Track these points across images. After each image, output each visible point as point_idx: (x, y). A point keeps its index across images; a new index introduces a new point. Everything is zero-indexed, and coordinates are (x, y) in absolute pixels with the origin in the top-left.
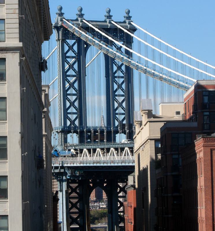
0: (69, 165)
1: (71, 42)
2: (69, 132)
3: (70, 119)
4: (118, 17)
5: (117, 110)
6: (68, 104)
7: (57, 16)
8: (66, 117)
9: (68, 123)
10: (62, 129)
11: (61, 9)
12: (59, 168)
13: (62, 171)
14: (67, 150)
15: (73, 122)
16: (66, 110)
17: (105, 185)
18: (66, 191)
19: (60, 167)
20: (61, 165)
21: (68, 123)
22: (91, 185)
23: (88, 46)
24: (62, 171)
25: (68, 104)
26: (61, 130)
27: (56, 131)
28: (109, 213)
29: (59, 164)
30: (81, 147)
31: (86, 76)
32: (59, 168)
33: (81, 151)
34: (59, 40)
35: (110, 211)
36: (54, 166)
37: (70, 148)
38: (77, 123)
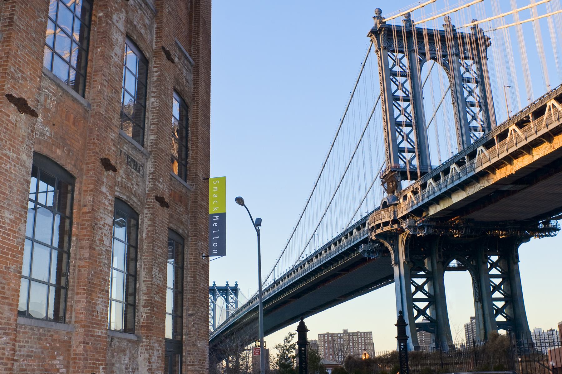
0: (405, 213)
9: (401, 162)
10: (391, 168)
11: (379, 11)
12: (390, 223)
14: (402, 197)
18: (404, 262)
20: (392, 218)
24: (396, 226)
28: (477, 302)
29: (390, 217)
31: (424, 98)
32: (390, 223)
33: (424, 186)
34: (380, 49)
35: (477, 298)
36: (383, 223)
38: (415, 162)
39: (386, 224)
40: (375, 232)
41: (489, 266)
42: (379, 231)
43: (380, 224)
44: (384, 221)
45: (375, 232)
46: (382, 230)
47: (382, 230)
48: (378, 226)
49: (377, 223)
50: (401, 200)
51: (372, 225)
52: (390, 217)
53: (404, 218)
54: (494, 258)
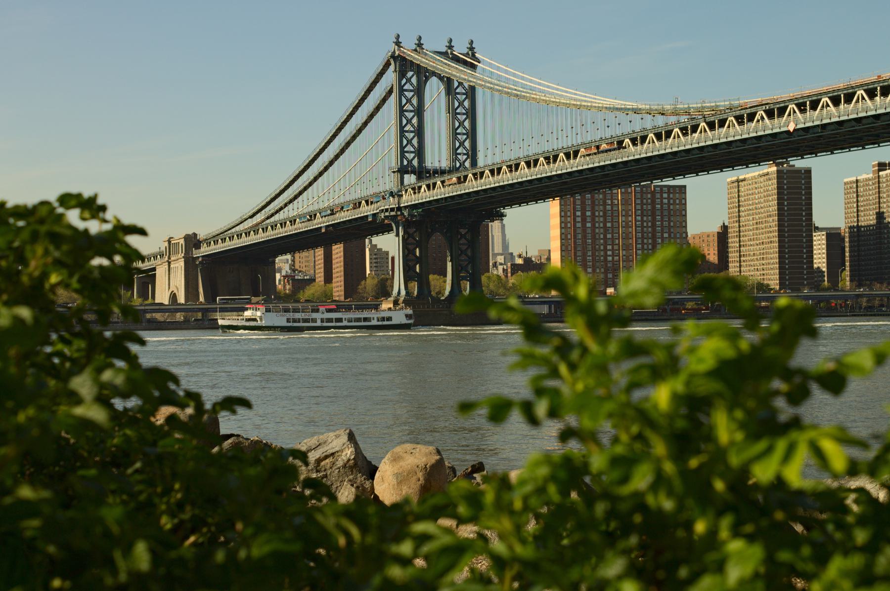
0: (406, 204)
2: (407, 172)
3: (406, 159)
4: (460, 49)
5: (464, 138)
6: (405, 142)
7: (394, 44)
8: (403, 156)
9: (405, 163)
15: (410, 162)
16: (402, 148)
17: (445, 231)
21: (405, 163)
22: (430, 230)
23: (427, 79)
25: (405, 142)
26: (397, 170)
27: (392, 171)
29: (396, 205)
30: (420, 184)
36: (391, 208)
37: (407, 188)
38: (415, 163)
39: (392, 210)
40: (384, 214)
41: (459, 237)
42: (387, 214)
43: (388, 209)
44: (391, 207)
45: (384, 214)
46: (390, 214)
47: (390, 214)
49: (386, 207)
50: (404, 193)
51: (382, 208)
52: (396, 205)
53: (406, 207)
54: (463, 231)
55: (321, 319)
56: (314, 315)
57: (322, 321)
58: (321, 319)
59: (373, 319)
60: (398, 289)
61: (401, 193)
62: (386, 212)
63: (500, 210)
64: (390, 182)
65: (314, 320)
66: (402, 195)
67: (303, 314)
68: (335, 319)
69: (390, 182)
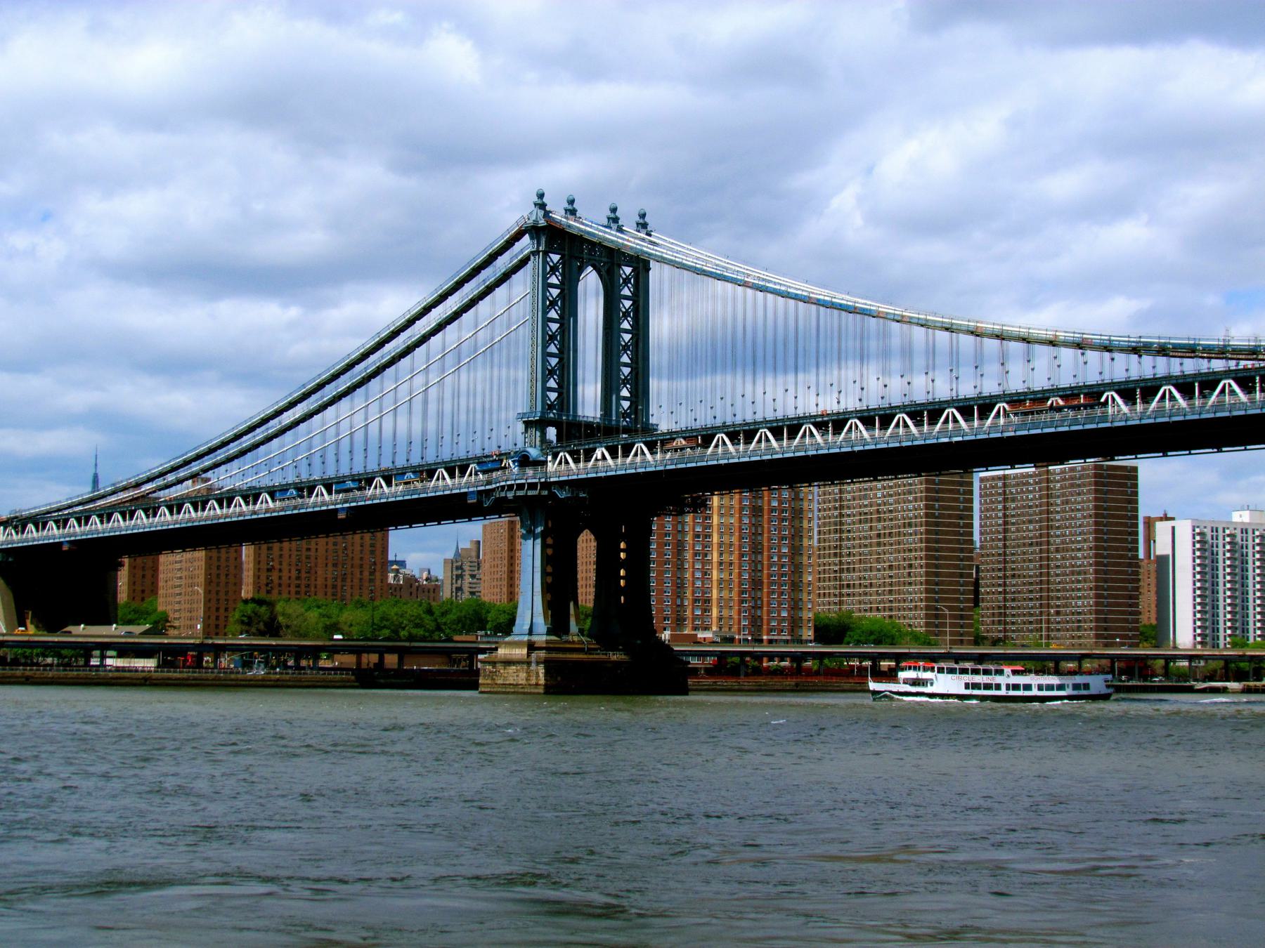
1: (555, 258)
13: (545, 493)
19: (541, 483)
20: (543, 480)
23: (581, 269)
24: (545, 493)
30: (591, 446)
36: (530, 484)
39: (532, 486)
44: (529, 481)
48: (521, 487)
55: (1038, 685)
56: (998, 679)
57: (1008, 687)
58: (1038, 685)
59: (1068, 686)
60: (529, 622)
61: (542, 459)
62: (508, 490)
63: (703, 495)
64: (513, 436)
65: (998, 687)
66: (544, 463)
67: (985, 677)
68: (1024, 685)
69: (513, 436)
